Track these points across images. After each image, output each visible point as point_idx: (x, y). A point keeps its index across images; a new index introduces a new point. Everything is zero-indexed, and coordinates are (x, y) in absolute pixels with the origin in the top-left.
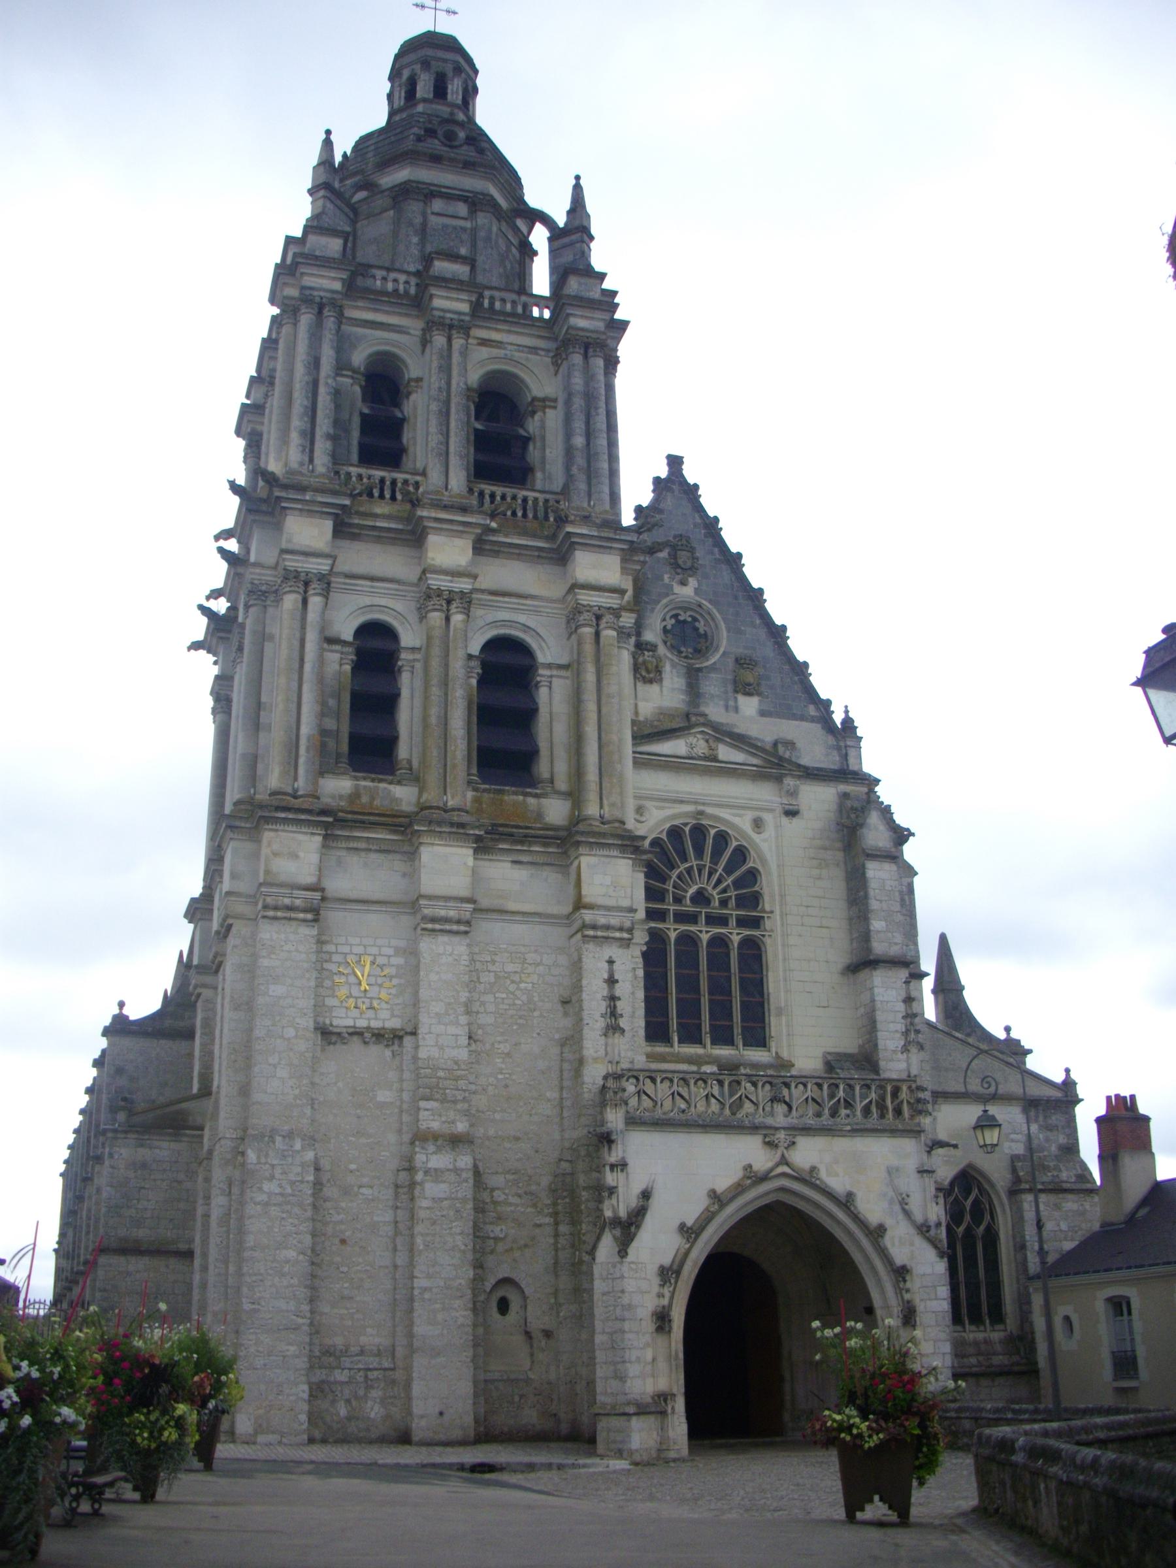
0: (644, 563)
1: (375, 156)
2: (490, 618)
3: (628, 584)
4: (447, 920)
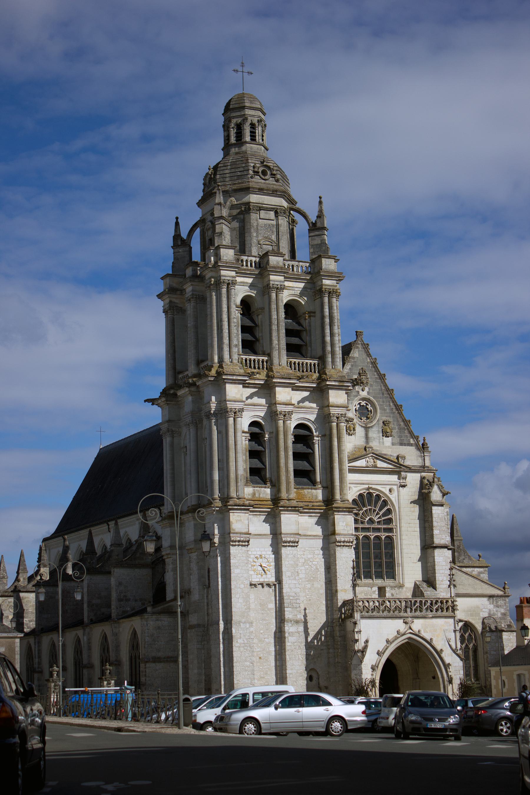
4: (289, 542)
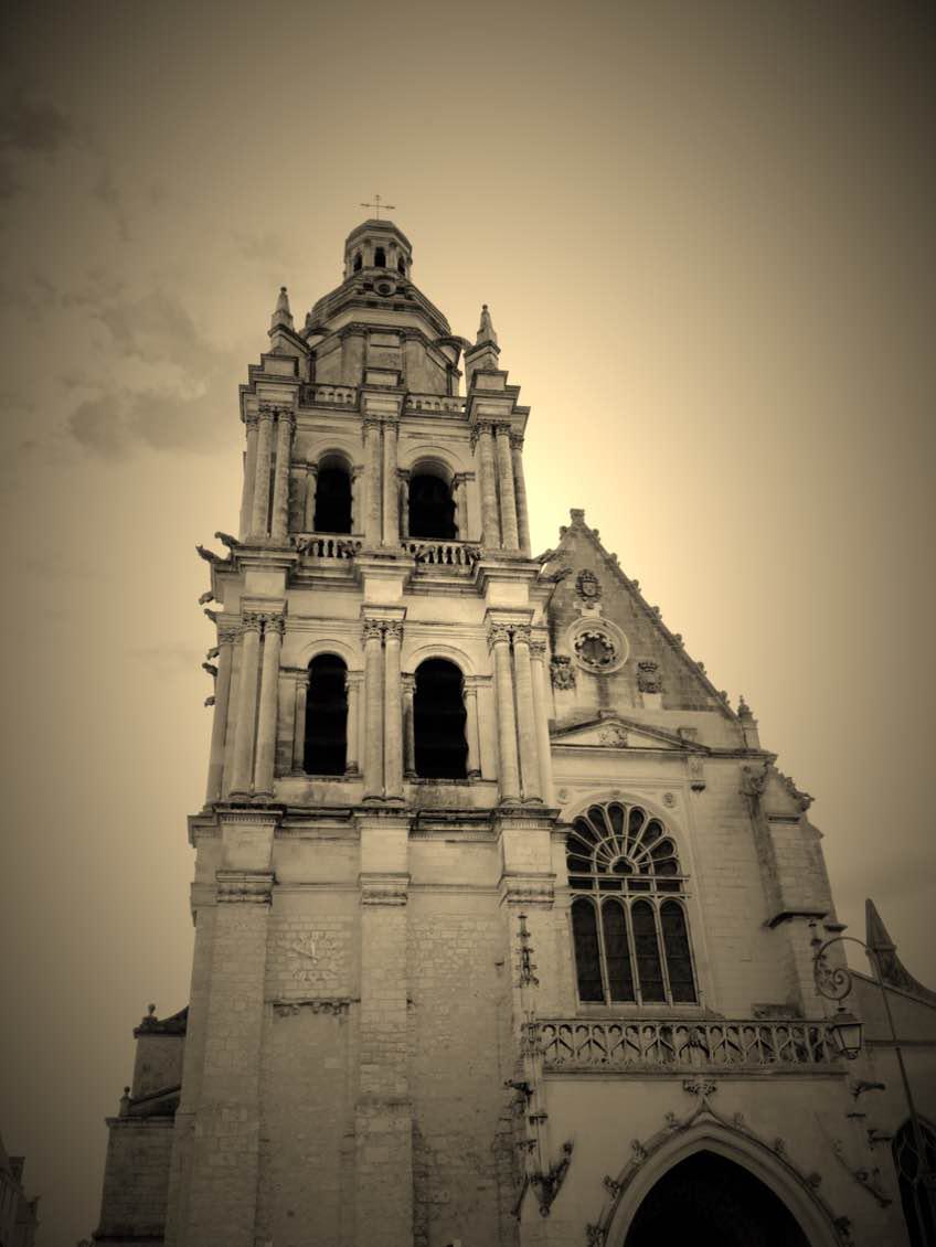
4: (385, 894)
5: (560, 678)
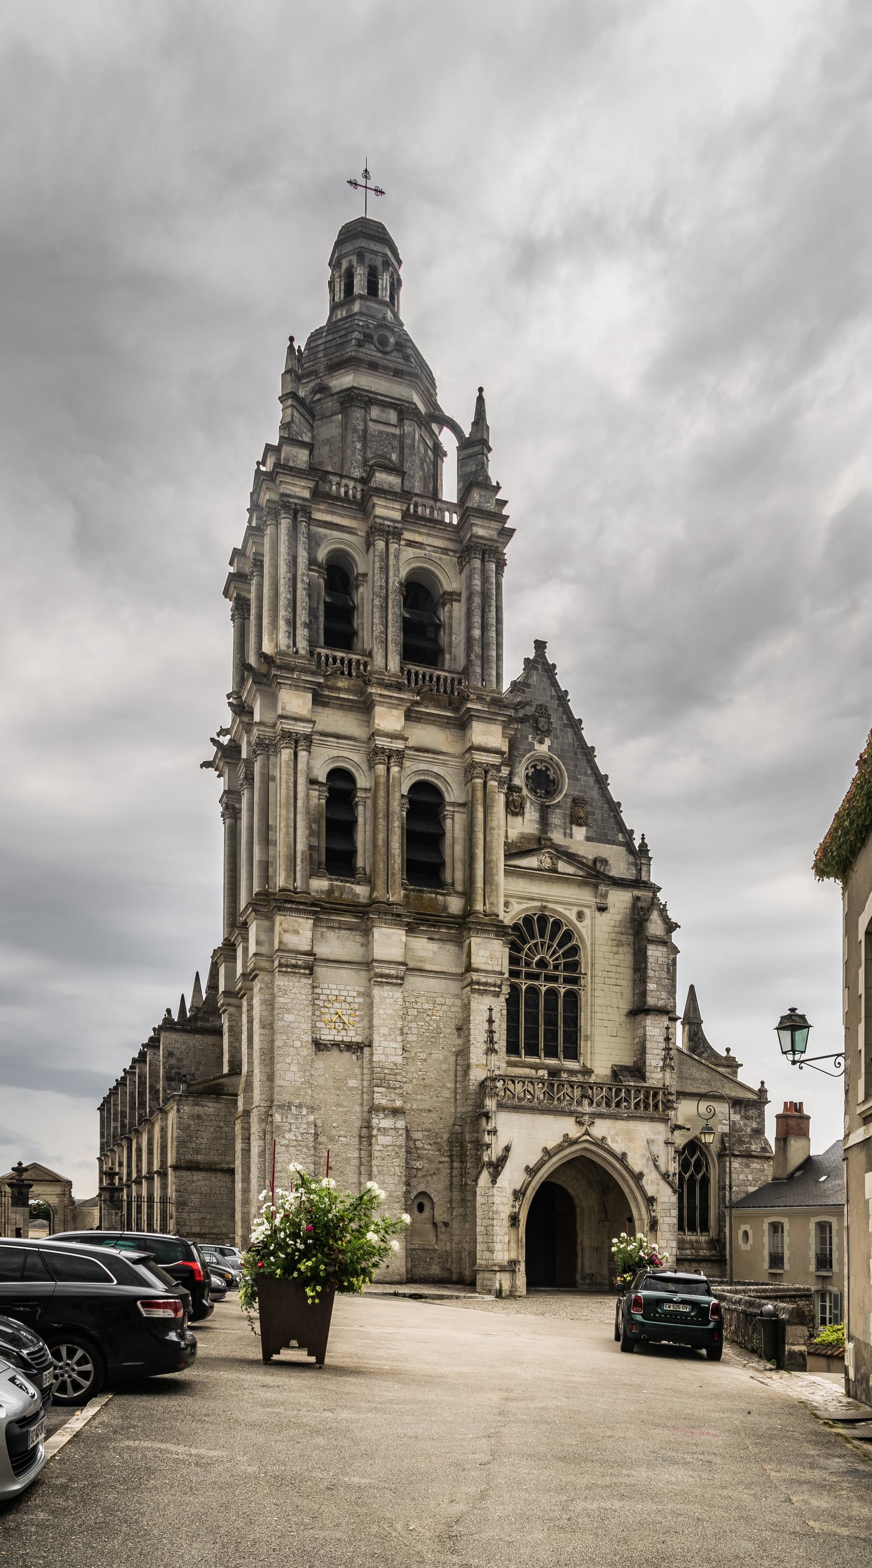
0: (516, 730)
1: (317, 352)
2: (414, 768)
3: (505, 749)
5: (514, 808)
